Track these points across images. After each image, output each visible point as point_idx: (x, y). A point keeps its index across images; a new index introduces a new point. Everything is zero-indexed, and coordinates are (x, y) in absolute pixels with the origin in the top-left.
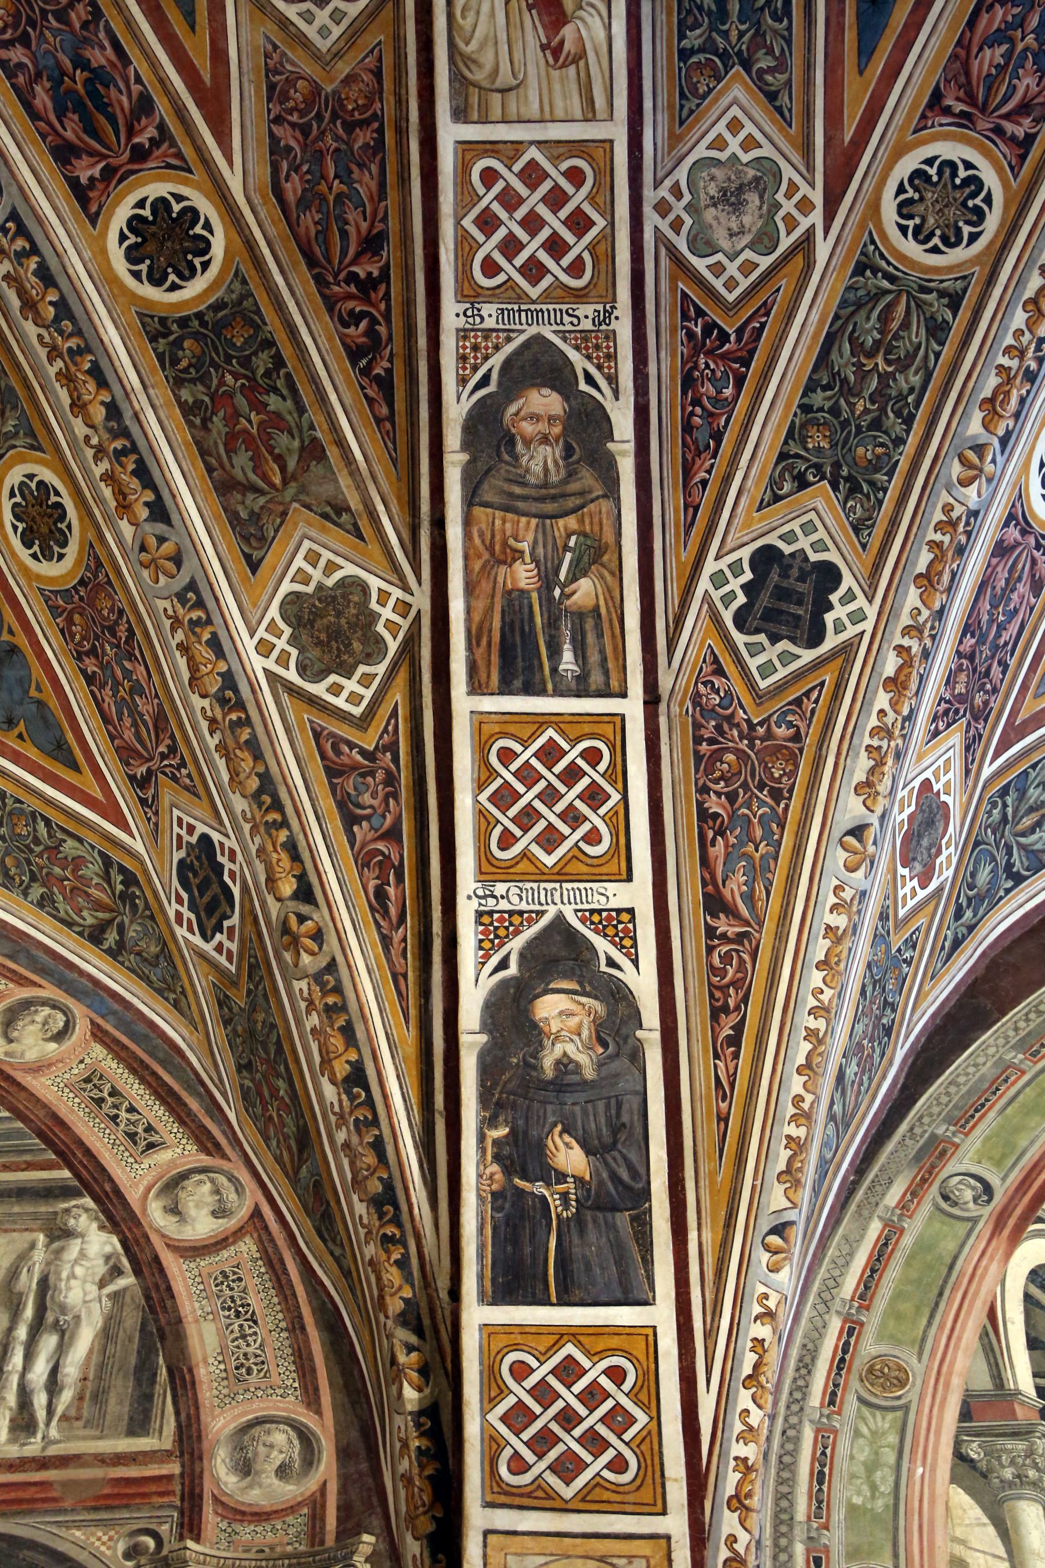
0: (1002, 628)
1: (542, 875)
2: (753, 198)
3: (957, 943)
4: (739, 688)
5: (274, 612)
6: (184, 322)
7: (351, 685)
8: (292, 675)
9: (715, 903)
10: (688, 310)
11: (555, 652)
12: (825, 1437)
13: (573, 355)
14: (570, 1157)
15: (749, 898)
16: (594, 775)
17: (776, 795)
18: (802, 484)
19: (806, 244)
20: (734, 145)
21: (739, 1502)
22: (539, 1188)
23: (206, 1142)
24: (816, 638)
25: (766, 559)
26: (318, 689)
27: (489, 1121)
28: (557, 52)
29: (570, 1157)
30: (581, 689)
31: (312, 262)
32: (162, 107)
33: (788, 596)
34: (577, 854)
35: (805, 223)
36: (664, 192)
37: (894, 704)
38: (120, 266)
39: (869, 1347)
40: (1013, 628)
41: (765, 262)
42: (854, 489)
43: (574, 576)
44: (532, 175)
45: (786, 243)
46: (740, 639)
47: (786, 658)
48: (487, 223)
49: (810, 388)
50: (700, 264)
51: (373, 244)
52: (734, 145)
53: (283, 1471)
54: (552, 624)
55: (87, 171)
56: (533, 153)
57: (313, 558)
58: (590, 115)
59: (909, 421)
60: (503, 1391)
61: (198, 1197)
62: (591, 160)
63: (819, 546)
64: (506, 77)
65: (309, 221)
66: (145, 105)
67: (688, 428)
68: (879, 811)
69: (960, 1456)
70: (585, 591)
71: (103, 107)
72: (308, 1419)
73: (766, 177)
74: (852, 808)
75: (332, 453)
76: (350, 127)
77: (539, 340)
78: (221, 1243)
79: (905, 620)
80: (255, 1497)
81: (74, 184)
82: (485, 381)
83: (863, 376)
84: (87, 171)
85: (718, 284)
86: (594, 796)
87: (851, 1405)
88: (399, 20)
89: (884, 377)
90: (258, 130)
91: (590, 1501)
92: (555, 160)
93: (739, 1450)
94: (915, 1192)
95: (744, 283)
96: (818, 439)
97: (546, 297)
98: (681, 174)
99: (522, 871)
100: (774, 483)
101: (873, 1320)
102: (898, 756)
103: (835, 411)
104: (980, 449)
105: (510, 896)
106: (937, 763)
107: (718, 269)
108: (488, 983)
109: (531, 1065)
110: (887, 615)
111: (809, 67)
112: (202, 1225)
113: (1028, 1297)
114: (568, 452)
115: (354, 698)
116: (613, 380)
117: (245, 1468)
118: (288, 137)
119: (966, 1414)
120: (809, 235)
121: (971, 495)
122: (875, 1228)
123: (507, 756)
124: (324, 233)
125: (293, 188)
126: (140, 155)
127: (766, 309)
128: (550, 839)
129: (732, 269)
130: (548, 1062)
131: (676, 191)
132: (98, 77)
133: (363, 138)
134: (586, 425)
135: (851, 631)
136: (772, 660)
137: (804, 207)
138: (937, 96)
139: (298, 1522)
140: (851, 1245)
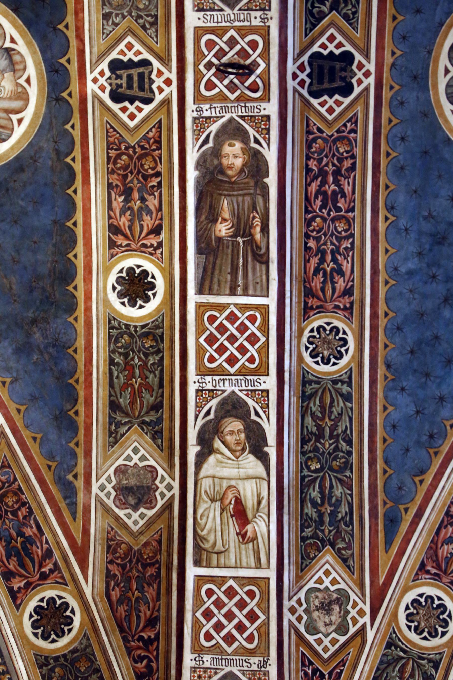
2: (336, 608)
6: (56, 659)
10: (304, 662)
19: (362, 631)
20: (327, 582)
28: (244, 536)
31: (122, 630)
32: (56, 554)
35: (361, 621)
36: (293, 602)
38: (28, 629)
41: (342, 639)
44: (230, 593)
45: (352, 630)
48: (208, 615)
50: (311, 639)
51: (152, 622)
52: (327, 582)
55: (17, 584)
56: (231, 582)
58: (259, 566)
62: (259, 587)
64: (219, 547)
65: (122, 610)
66: (49, 554)
71: (29, 555)
73: (342, 598)
76: (145, 566)
77: (231, 674)
81: (11, 590)
84: (17, 584)
85: (319, 649)
88: (171, 518)
90: (101, 566)
92: (242, 586)
95: (333, 649)
97: (235, 652)
98: (302, 595)
107: (319, 641)
111: (362, 548)
118: (115, 570)
120: (364, 627)
124: (128, 616)
125: (115, 594)
126: (44, 577)
127: (343, 663)
129: (326, 642)
131: (299, 602)
132: (28, 541)
133: (150, 571)
137: (361, 613)
138: (422, 566)
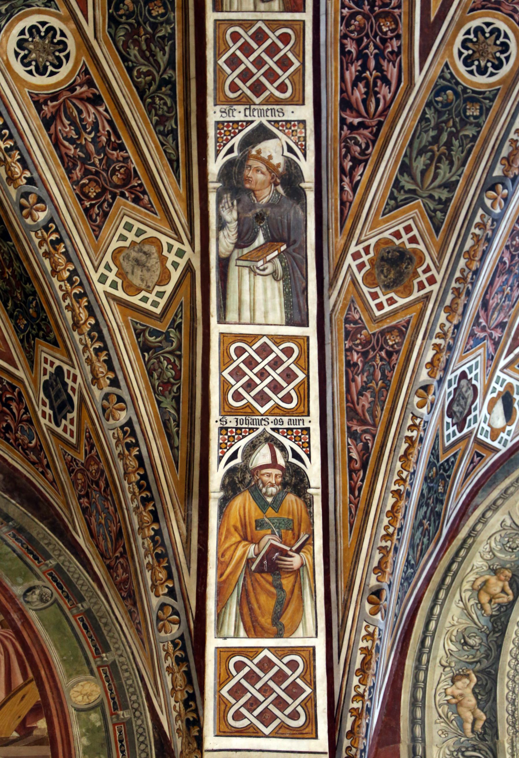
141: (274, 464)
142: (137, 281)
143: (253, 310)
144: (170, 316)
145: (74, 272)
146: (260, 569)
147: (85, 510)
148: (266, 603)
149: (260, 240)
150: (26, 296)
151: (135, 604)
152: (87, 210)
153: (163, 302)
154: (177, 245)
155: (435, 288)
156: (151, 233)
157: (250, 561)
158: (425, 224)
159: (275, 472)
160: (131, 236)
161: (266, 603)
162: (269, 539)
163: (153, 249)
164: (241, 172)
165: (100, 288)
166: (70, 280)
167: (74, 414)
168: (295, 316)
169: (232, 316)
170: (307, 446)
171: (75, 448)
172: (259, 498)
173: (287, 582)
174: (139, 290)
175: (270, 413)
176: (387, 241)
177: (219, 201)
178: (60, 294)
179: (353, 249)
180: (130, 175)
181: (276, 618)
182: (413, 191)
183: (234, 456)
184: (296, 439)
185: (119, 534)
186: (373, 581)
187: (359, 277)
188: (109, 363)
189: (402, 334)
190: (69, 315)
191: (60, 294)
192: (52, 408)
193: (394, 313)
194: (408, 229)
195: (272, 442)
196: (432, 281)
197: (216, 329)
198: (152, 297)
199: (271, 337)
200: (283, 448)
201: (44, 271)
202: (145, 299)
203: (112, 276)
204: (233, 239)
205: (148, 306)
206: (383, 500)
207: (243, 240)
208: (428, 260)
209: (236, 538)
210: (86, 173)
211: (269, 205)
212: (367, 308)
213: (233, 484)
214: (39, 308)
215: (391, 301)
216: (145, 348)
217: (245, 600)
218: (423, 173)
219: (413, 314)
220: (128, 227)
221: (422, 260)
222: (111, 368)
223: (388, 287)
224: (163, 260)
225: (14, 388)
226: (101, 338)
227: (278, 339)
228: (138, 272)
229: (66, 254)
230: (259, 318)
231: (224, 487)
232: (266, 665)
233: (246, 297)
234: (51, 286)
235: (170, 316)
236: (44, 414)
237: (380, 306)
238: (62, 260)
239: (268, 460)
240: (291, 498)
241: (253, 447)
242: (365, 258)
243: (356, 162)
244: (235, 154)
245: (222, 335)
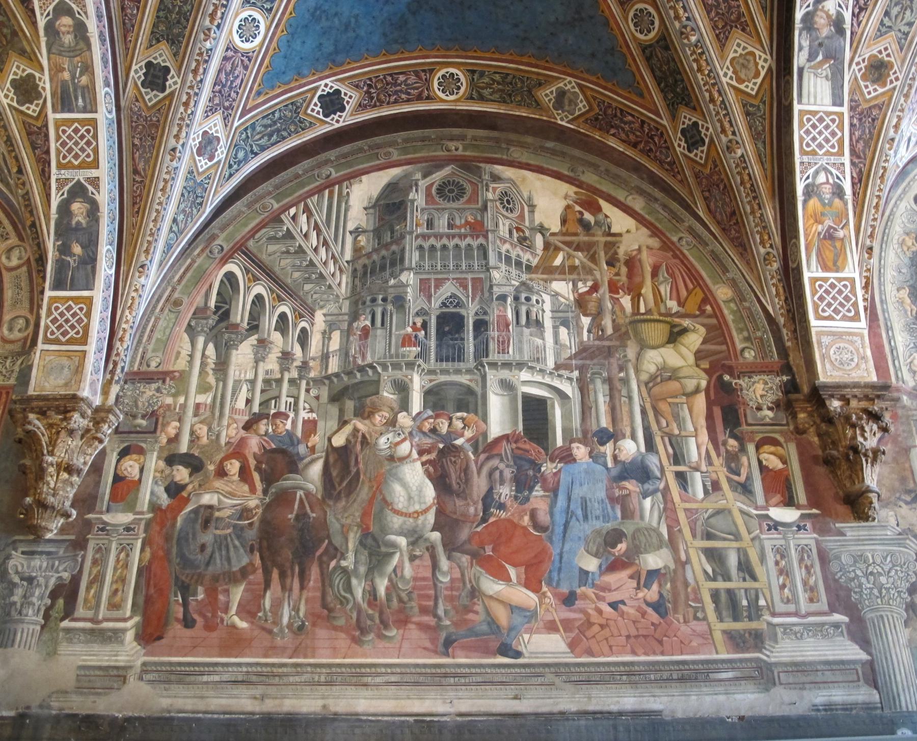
0: (232, 82)
1: (74, 167)
3: (231, 175)
4: (142, 105)
5: (8, 85)
7: (33, 107)
8: (15, 104)
9: (136, 172)
11: (76, 99)
12: (157, 319)
13: (74, 6)
14: (77, 249)
15: (144, 170)
16: (88, 137)
17: (153, 139)
18: (158, 41)
21: (121, 340)
22: (68, 259)
23: (21, 239)
24: (163, 90)
25: (149, 65)
26: (23, 108)
27: (56, 240)
29: (77, 249)
30: (85, 110)
33: (156, 77)
34: (84, 161)
37: (186, 110)
39: (176, 295)
40: (238, 81)
42: (173, 43)
43: (81, 76)
46: (143, 90)
47: (156, 96)
49: (158, 11)
53: (20, 331)
54: (75, 90)
57: (18, 67)
59: (188, 21)
60: (52, 314)
61: (16, 253)
63: (164, 61)
67: (124, 24)
68: (181, 142)
69: (189, 325)
70: (84, 80)
72: (29, 316)
74: (172, 142)
75: (20, 34)
78: (18, 267)
79: (189, 84)
80: (12, 337)
82: (48, 15)
83: (174, 6)
86: (88, 143)
87: (166, 311)
89: (180, 7)
91: (68, 342)
93: (124, 326)
94: (202, 251)
96: (162, 27)
99: (69, 166)
100: (150, 41)
101: (179, 288)
102: (188, 126)
103: (166, 18)
104: (209, 30)
105: (66, 174)
106: (216, 125)
108: (59, 200)
109: (69, 223)
110: (184, 82)
112: (15, 262)
113: (222, 281)
114: (76, 37)
115: (34, 111)
116: (86, 13)
117: (11, 329)
119: (194, 314)
121: (208, 45)
122: (189, 261)
123: (64, 132)
128: (76, 156)
130: (74, 223)
134: (80, 29)
135: (174, 87)
136: (152, 97)
139: (20, 343)
140: (181, 265)
141: (827, 182)
142: (743, 76)
143: (815, 98)
144: (760, 96)
145: (710, 71)
146: (825, 238)
147: (706, 199)
148: (829, 255)
149: (820, 58)
150: (676, 81)
151: (745, 250)
152: (717, 36)
153: (756, 88)
154: (764, 56)
155: (899, 83)
156: (750, 49)
157: (819, 234)
158: (895, 46)
159: (828, 186)
160: (740, 51)
161: (829, 255)
162: (828, 222)
163: (751, 58)
164: (812, 18)
165: (724, 80)
166: (708, 75)
167: (705, 148)
168: (837, 100)
169: (805, 100)
170: (843, 172)
171: (704, 166)
172: (821, 200)
173: (838, 244)
174: (744, 81)
175: (825, 154)
176: (875, 56)
177: (800, 35)
178: (702, 83)
179: (856, 60)
180: (740, 15)
181: (835, 263)
182: (890, 27)
183: (808, 178)
184: (838, 169)
185: (733, 213)
186: (868, 243)
187: (859, 76)
188: (730, 122)
189: (880, 109)
190: (707, 95)
191: (702, 83)
192: (686, 142)
193: (876, 97)
194: (886, 49)
195: (825, 169)
196: (897, 79)
197: (797, 107)
198: (751, 85)
199: (825, 113)
200: (831, 174)
201: (691, 68)
202: (747, 87)
203: (730, 73)
204: (806, 56)
205: (748, 90)
206: (871, 200)
207: (812, 57)
208: (896, 67)
209: (812, 221)
210: (717, 14)
211: (827, 37)
212: (862, 94)
213: (810, 191)
214: (685, 89)
215: (875, 90)
216: (747, 114)
217: (819, 254)
218: (896, 17)
219: (886, 98)
220: (739, 45)
221: (892, 67)
222: (731, 125)
223: (874, 82)
224: (756, 64)
225: (657, 129)
226: (726, 108)
227: (828, 114)
228: (744, 71)
229: (706, 60)
230: (819, 102)
231: (804, 194)
232: (833, 286)
233: (812, 90)
234: (696, 78)
235: (760, 96)
236: (679, 146)
237: (869, 93)
238: (704, 64)
239: (824, 180)
240: (837, 201)
241: (817, 173)
242: (862, 65)
243: (861, 9)
244: (811, 8)
245: (800, 111)
